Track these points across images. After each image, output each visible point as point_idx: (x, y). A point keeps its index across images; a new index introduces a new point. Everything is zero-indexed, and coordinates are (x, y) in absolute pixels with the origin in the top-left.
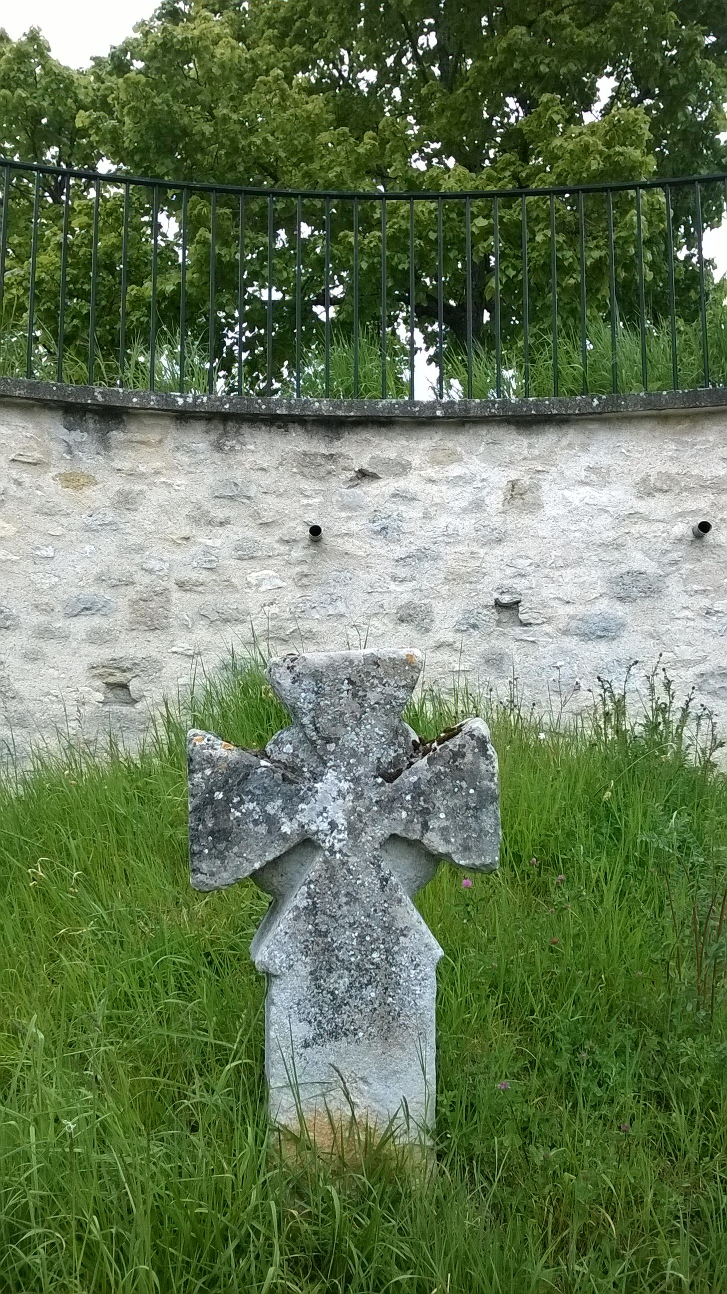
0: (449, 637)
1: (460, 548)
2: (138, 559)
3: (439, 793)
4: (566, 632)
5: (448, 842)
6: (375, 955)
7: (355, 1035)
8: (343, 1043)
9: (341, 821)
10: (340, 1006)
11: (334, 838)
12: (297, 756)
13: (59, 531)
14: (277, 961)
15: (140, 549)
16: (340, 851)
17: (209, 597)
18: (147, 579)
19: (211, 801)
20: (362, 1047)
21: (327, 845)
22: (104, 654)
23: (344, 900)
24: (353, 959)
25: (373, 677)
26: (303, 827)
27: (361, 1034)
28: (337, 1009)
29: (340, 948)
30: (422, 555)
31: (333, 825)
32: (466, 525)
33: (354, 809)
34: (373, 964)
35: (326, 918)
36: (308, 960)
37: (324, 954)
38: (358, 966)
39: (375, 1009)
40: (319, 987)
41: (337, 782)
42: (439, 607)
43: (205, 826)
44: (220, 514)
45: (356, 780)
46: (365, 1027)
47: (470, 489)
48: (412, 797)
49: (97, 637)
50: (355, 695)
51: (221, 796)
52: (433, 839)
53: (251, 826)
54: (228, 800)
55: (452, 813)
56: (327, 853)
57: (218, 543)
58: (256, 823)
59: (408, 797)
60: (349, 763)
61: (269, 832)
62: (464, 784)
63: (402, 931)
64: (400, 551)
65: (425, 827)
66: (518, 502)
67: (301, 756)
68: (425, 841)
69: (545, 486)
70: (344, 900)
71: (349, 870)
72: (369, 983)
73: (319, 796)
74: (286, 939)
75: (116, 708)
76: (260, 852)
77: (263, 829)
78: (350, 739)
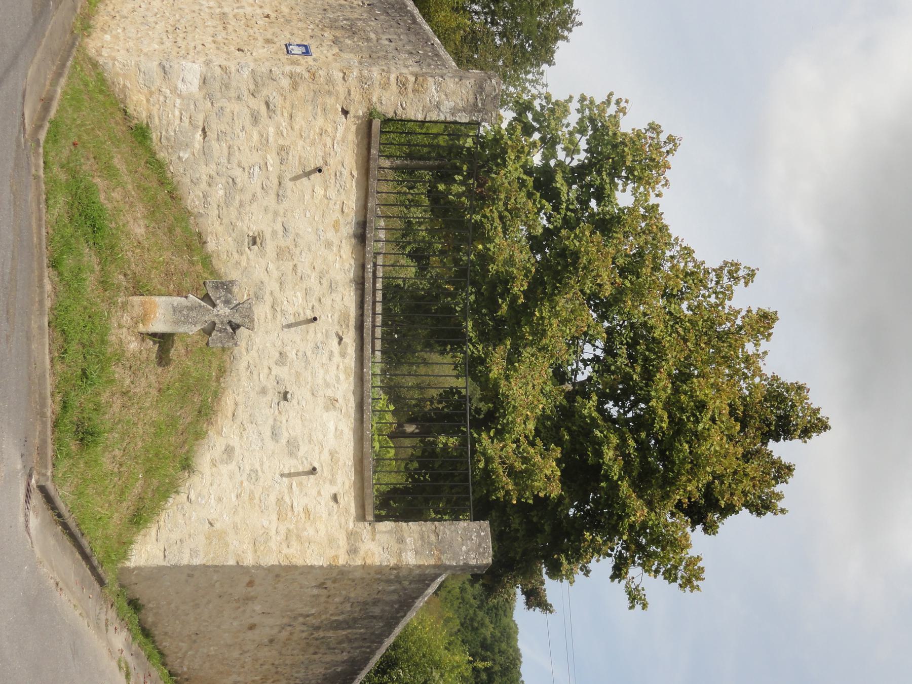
0: (274, 373)
1: (310, 378)
2: (306, 249)
4: (275, 420)
13: (316, 219)
15: (310, 250)
17: (290, 277)
18: (298, 252)
22: (268, 236)
30: (307, 361)
32: (320, 381)
42: (285, 369)
44: (324, 281)
47: (335, 383)
49: (274, 233)
57: (312, 281)
64: (309, 354)
66: (329, 402)
69: (335, 413)
75: (247, 240)
78: (237, 315)
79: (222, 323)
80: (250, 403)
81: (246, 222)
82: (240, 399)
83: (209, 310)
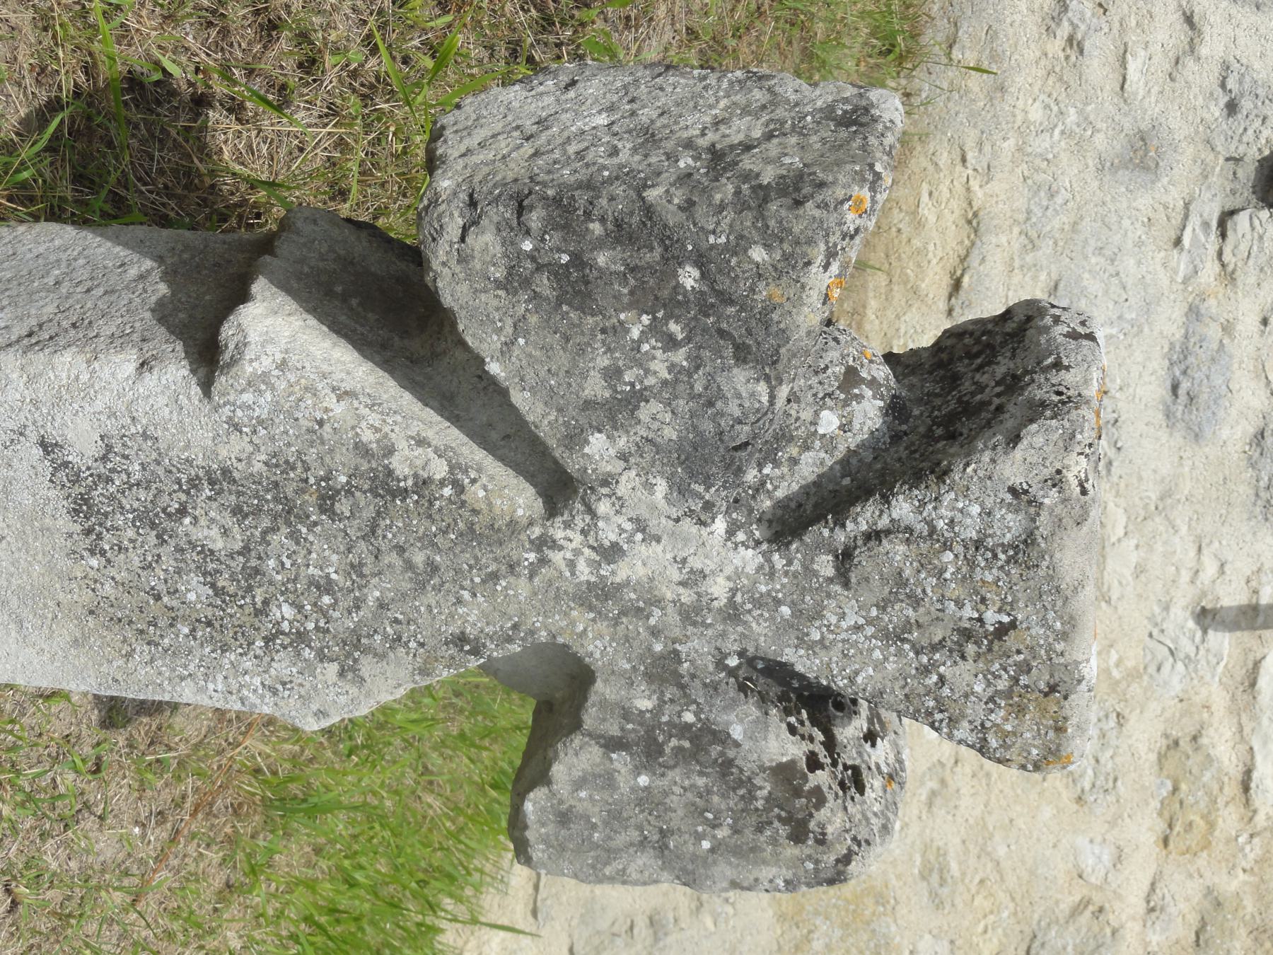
0: (1212, 48)
3: (701, 782)
4: (1194, 313)
5: (579, 784)
6: (288, 612)
7: (92, 553)
8: (65, 523)
9: (622, 571)
10: (153, 526)
11: (577, 552)
12: (806, 447)
14: (248, 397)
16: (543, 561)
19: (672, 260)
20: (64, 564)
21: (559, 534)
23: (419, 558)
24: (272, 563)
25: (1016, 680)
26: (605, 483)
27: (94, 562)
28: (145, 519)
29: (295, 536)
31: (612, 553)
33: (658, 602)
34: (266, 602)
35: (369, 513)
36: (258, 467)
37: (276, 500)
38: (257, 571)
39: (158, 598)
40: (194, 483)
41: (729, 570)
43: (600, 244)
45: (732, 613)
46: (113, 572)
48: (688, 726)
50: (967, 634)
51: (689, 283)
52: (584, 756)
53: (603, 361)
54: (675, 303)
56: (536, 531)
58: (613, 374)
59: (689, 717)
60: (778, 602)
61: (588, 405)
62: (722, 833)
63: (354, 670)
65: (612, 744)
67: (808, 457)
68: (577, 740)
70: (419, 558)
71: (494, 577)
72: (219, 592)
73: (688, 526)
74: (305, 423)
76: (530, 377)
77: (595, 387)
78: (846, 613)
79: (664, 671)
80: (1059, 221)
82: (1001, 196)
83: (485, 533)
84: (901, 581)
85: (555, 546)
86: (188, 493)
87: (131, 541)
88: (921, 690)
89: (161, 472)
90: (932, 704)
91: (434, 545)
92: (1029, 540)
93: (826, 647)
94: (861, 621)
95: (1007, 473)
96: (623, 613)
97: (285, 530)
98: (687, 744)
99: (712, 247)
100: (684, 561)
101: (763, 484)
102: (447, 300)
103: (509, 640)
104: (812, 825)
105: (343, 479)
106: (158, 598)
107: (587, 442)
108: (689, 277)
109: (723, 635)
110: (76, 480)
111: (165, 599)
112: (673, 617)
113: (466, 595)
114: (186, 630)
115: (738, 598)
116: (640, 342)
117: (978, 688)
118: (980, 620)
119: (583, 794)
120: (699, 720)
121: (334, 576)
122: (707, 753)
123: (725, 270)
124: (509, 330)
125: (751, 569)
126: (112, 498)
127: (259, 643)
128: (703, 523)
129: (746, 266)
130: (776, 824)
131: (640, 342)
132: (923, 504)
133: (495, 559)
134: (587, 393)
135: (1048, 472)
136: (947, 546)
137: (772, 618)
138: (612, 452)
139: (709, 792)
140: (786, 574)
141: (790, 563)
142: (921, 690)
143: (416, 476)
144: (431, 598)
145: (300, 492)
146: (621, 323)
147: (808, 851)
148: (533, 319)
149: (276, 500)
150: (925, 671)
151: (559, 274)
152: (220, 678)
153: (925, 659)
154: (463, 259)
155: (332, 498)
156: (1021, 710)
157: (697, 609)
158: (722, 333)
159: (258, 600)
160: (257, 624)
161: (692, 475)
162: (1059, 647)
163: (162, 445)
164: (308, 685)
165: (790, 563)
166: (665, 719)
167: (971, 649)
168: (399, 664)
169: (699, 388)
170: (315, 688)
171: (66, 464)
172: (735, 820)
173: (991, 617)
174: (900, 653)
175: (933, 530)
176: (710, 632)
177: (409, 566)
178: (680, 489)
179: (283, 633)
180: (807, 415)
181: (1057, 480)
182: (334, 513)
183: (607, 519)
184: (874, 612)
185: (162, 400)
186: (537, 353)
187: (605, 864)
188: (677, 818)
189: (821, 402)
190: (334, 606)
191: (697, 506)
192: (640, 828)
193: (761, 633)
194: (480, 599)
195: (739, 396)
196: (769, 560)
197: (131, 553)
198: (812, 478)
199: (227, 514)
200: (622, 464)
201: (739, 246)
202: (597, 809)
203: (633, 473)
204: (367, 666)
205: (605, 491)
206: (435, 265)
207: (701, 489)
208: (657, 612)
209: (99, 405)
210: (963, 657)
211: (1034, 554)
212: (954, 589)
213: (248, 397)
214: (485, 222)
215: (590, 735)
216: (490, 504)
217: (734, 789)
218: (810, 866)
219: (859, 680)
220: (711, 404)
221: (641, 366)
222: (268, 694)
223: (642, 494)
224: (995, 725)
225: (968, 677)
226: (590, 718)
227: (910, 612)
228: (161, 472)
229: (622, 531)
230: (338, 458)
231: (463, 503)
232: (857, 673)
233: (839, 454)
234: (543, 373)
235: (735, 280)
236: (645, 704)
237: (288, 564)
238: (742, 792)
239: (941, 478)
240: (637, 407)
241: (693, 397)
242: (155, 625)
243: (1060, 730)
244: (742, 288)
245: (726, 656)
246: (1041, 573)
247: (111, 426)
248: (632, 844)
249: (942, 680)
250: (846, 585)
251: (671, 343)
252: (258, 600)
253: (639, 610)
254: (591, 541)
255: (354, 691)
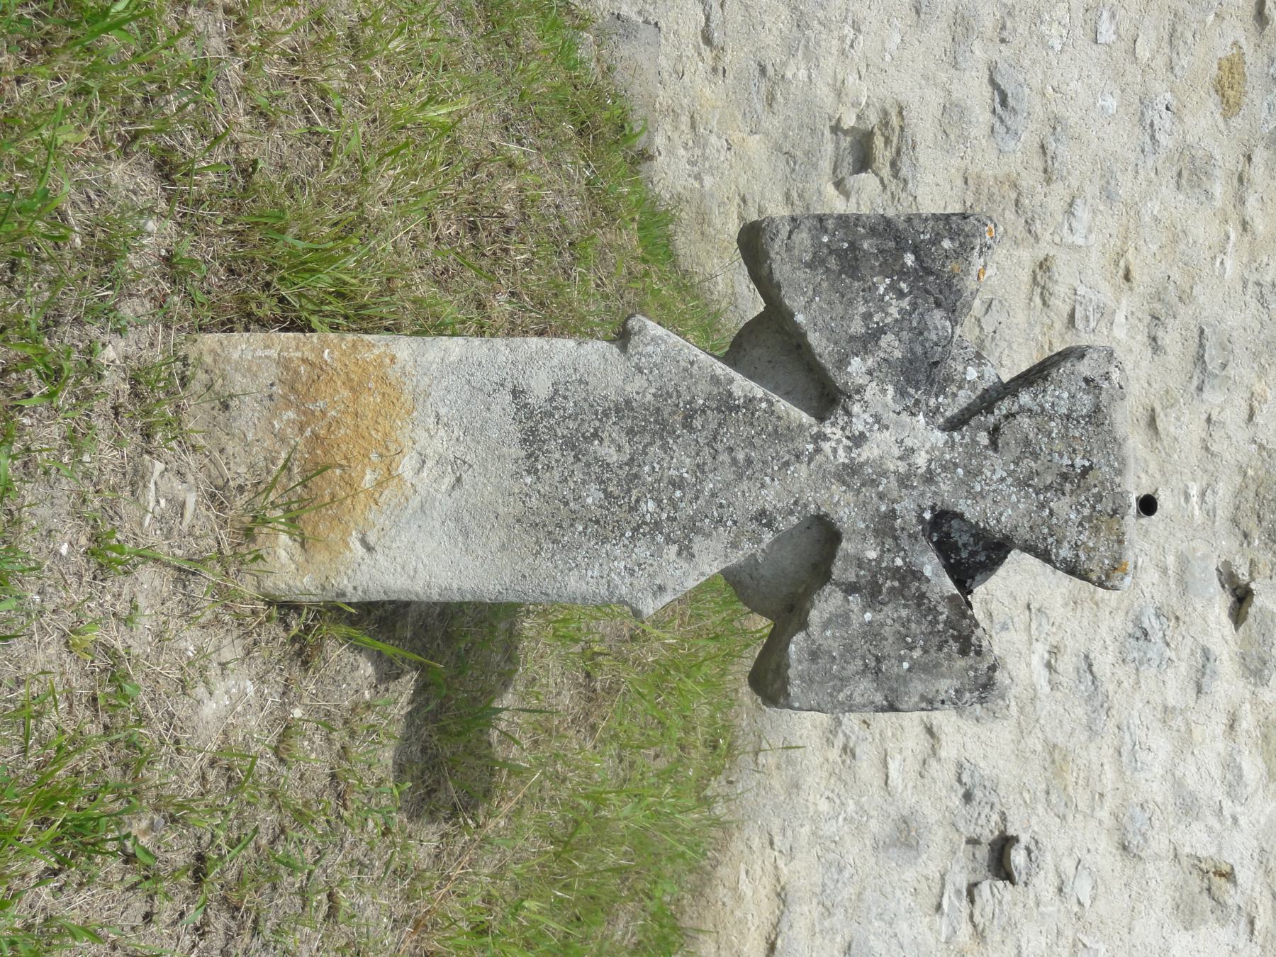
0: (948, 751)
1: (1110, 773)
2: (1092, 190)
3: (904, 613)
5: (826, 625)
6: (651, 506)
7: (529, 472)
8: (517, 451)
9: (867, 453)
10: (573, 448)
11: (839, 441)
12: (960, 387)
13: (1143, 52)
14: (650, 349)
15: (1108, 195)
16: (818, 450)
17: (1020, 317)
18: (1056, 205)
19: (901, 249)
20: (507, 482)
21: (828, 430)
22: (924, 127)
23: (741, 456)
24: (647, 469)
25: (1093, 507)
26: (858, 392)
27: (529, 480)
28: (570, 444)
29: (665, 447)
30: (1097, 700)
31: (859, 440)
32: (1155, 788)
33: (884, 474)
34: (638, 501)
35: (713, 426)
36: (649, 397)
37: (656, 422)
38: (636, 476)
39: (566, 504)
40: (606, 414)
41: (928, 445)
42: (1001, 733)
43: (864, 237)
44: (1170, 338)
45: (929, 478)
46: (539, 486)
47: (1219, 794)
48: (899, 568)
49: (953, 112)
50: (1065, 477)
51: (909, 263)
52: (832, 601)
53: (862, 309)
54: (903, 273)
55: (872, 633)
56: (815, 430)
57: (1120, 333)
58: (867, 317)
59: (899, 562)
60: (956, 465)
61: (852, 338)
62: (916, 654)
63: (688, 548)
64: (1104, 664)
65: (850, 589)
66: (1195, 883)
67: (961, 393)
68: (828, 588)
69: (1224, 935)
70: (741, 456)
71: (787, 464)
72: (608, 495)
73: (905, 417)
74: (682, 364)
75: (829, 148)
76: (820, 323)
77: (857, 327)
78: (996, 468)
79: (885, 527)
80: (849, 892)
81: (830, 63)
82: (802, 873)
83: (783, 433)
84: (1027, 442)
85: (826, 438)
86: (601, 420)
87: (557, 461)
88: (1040, 522)
89: (586, 406)
90: (1046, 531)
91: (752, 444)
92: (1097, 409)
93: (983, 497)
94: (1005, 474)
95: (1082, 369)
96: (863, 485)
97: (659, 443)
98: (896, 584)
99: (922, 241)
100: (902, 441)
101: (938, 408)
102: (777, 275)
103: (791, 513)
104: (973, 639)
105: (701, 402)
106: (566, 504)
107: (849, 363)
108: (909, 259)
109: (922, 494)
110: (530, 416)
111: (571, 504)
112: (894, 484)
113: (767, 479)
114: (581, 528)
115: (933, 466)
116: (884, 295)
117: (1073, 516)
118: (1072, 465)
119: (828, 633)
120: (905, 563)
121: (685, 475)
122: (909, 588)
123: (929, 254)
124: (811, 293)
125: (940, 444)
126: (551, 428)
127: (628, 534)
128: (913, 414)
129: (940, 252)
130: (951, 642)
131: (884, 295)
132: (1035, 395)
133: (788, 452)
134: (852, 330)
135: (1102, 372)
136: (1051, 419)
137: (952, 478)
138: (864, 370)
139: (909, 621)
140: (961, 445)
141: (963, 438)
142: (1040, 522)
143: (745, 396)
144: (745, 485)
145: (672, 413)
146: (874, 284)
147: (970, 662)
148: (825, 285)
149: (656, 422)
150: (1042, 506)
151: (840, 254)
152: (597, 566)
153: (1042, 497)
154: (789, 249)
155: (691, 417)
156: (1097, 530)
157: (908, 476)
158: (927, 292)
159: (633, 499)
160: (629, 518)
161: (908, 381)
162: (1117, 480)
163: (590, 388)
164: (655, 564)
165: (963, 438)
166: (884, 565)
167: (1068, 487)
168: (718, 540)
169: (915, 324)
170: (660, 566)
171: (526, 405)
172: (925, 642)
173: (1079, 462)
174: (1027, 496)
175: (1043, 409)
176: (914, 493)
177: (734, 461)
178: (901, 392)
179: (646, 523)
180: (960, 368)
181: (1107, 377)
182: (692, 428)
183: (858, 416)
184: (1012, 467)
185: (595, 357)
186: (825, 306)
187: (840, 691)
188: (888, 647)
189: (967, 362)
190: (681, 499)
191: (910, 403)
192: (863, 658)
193: (946, 491)
194: (777, 482)
195: (936, 328)
196: (951, 437)
197: (555, 472)
198: (965, 405)
199: (623, 435)
200: (869, 377)
201: (936, 241)
202: (836, 645)
203: (874, 384)
204: (698, 544)
205: (857, 397)
206: (772, 255)
207: (912, 391)
208: (884, 481)
209: (555, 362)
210: (1064, 494)
211: (1100, 417)
212: (1058, 445)
213: (650, 349)
214: (802, 227)
215: (837, 584)
216: (788, 414)
217: (925, 616)
218: (972, 674)
219: (1003, 519)
220: (921, 333)
221: (883, 311)
222: (627, 575)
223: (879, 397)
224: (1084, 543)
225: (1067, 508)
226: (837, 570)
227: (1032, 464)
228: (586, 406)
229: (867, 423)
230: (699, 387)
231: (773, 412)
232: (1001, 514)
233: (979, 392)
234: (828, 318)
235: (934, 260)
236: (872, 555)
237: (657, 467)
238: (929, 618)
239: (1045, 379)
240: (879, 338)
241: (911, 329)
242: (561, 527)
243: (1120, 542)
244: (937, 266)
245: (923, 510)
246: (1106, 428)
247: (561, 375)
248: (857, 673)
249: (1051, 513)
250: (996, 450)
251: (901, 295)
252: (633, 499)
253: (873, 480)
254: (848, 433)
255: (685, 565)
